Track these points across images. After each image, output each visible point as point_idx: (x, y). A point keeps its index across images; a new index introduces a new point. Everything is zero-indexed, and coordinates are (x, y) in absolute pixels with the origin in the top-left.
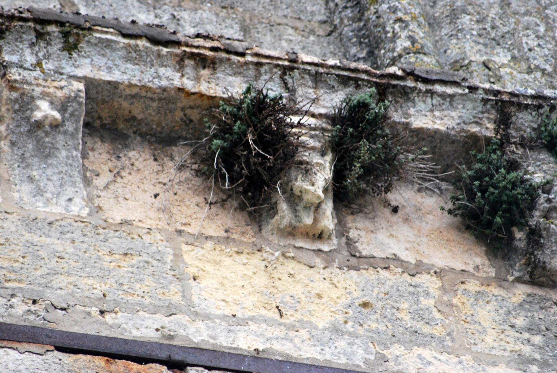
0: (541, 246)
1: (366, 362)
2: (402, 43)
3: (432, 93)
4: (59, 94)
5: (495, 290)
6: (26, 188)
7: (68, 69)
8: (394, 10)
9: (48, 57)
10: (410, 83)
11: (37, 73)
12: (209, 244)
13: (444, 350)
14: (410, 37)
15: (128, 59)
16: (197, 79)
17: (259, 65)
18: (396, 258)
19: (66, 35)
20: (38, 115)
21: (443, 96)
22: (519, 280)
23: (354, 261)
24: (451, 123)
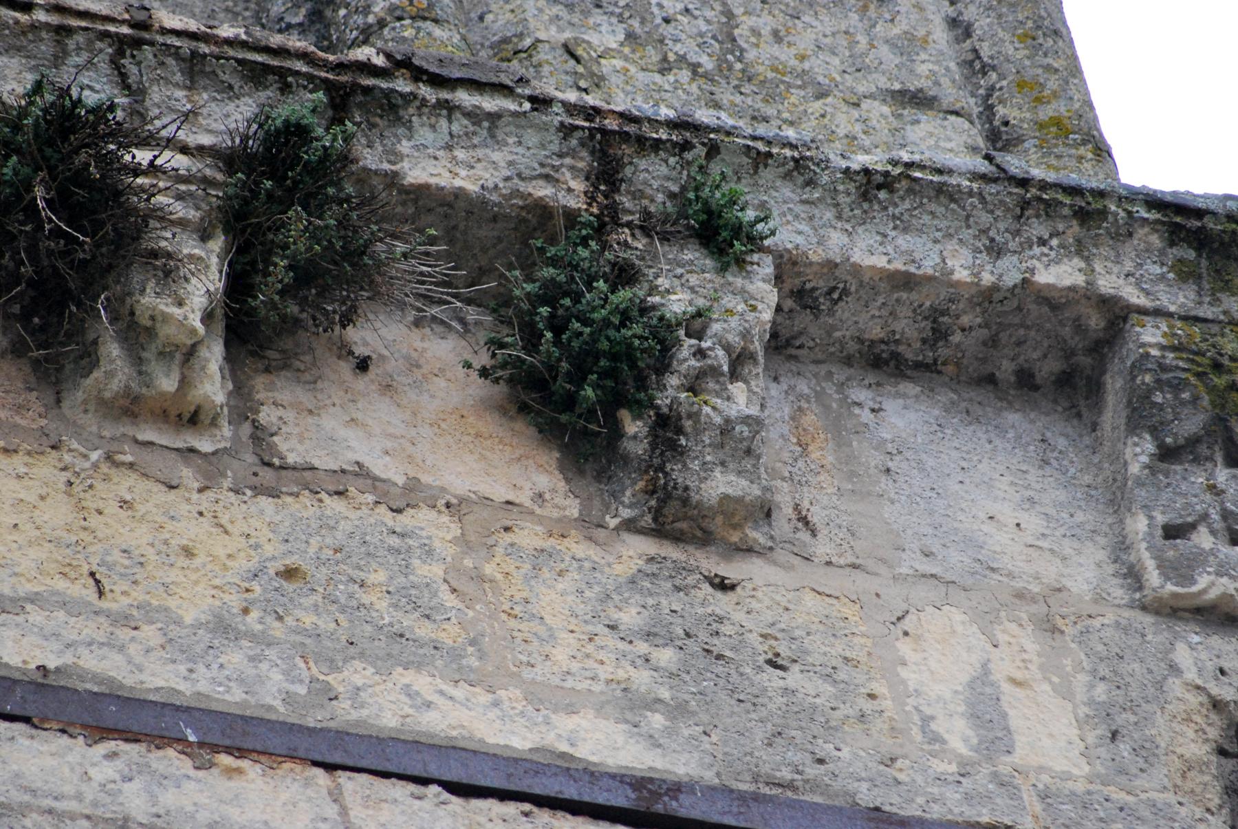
3: (449, 108)
5: (578, 547)
10: (403, 85)
17: (62, 31)
18: (361, 472)
21: (475, 116)
22: (630, 526)
23: (267, 475)
24: (491, 177)
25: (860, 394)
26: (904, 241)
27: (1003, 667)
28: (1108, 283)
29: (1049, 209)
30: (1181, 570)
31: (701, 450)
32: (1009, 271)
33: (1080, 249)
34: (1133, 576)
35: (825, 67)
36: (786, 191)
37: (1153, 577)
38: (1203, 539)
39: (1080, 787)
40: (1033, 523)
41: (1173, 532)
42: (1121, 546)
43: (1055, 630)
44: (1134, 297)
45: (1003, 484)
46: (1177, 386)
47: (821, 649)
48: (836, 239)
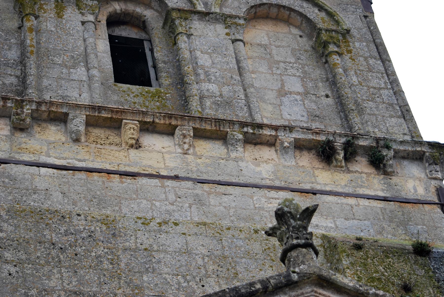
0: (386, 167)
1: (352, 192)
2: (357, 128)
3: (363, 138)
4: (289, 141)
5: (377, 176)
6: (283, 160)
7: (290, 136)
8: (355, 122)
9: (286, 134)
10: (359, 136)
11: (284, 137)
12: (320, 170)
13: (367, 188)
14: (358, 127)
15: (302, 133)
16: (316, 137)
17: (328, 133)
18: (357, 171)
19: (290, 129)
20: (285, 145)
21: (365, 138)
22: (382, 174)
23: (349, 172)
24: (367, 144)
25: (402, 161)
26: (405, 147)
27: (416, 185)
28: (423, 149)
29: (418, 143)
30: (431, 175)
31: (388, 167)
32: (414, 149)
33: (420, 147)
34: (427, 176)
35: (396, 132)
36: (394, 143)
37: (429, 176)
38: (433, 172)
39: (424, 195)
40: (418, 171)
41: (431, 171)
42: (426, 173)
43: (420, 181)
44: (426, 151)
45: (415, 168)
46: (430, 158)
47: (400, 184)
48: (399, 147)
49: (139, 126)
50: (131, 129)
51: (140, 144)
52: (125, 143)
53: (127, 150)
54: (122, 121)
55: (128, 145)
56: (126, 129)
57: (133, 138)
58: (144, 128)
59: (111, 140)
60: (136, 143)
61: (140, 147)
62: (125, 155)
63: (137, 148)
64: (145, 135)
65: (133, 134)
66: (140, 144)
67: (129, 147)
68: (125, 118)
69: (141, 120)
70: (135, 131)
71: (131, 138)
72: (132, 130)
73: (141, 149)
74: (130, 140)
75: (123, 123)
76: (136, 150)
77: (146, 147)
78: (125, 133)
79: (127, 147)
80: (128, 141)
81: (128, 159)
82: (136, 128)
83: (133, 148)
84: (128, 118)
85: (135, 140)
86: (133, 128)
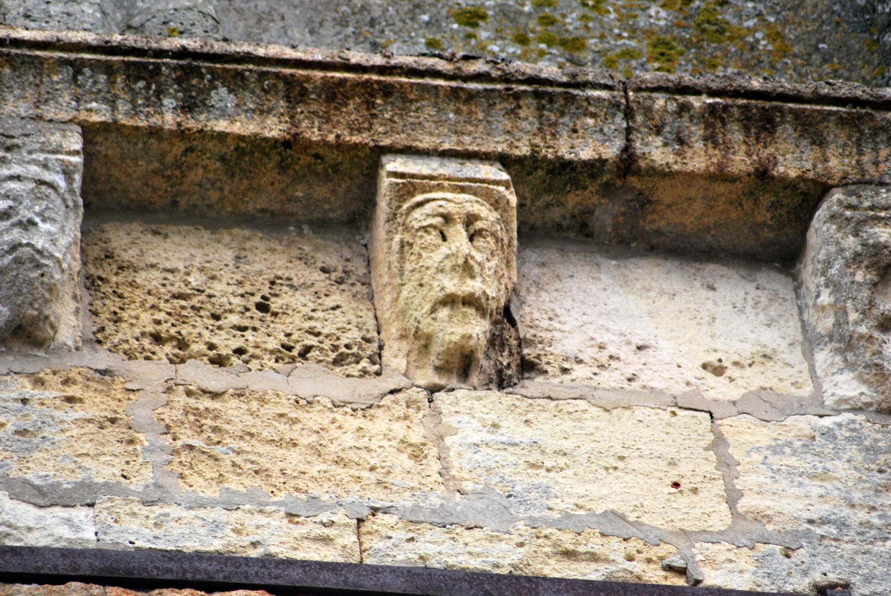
49: (513, 200)
50: (450, 232)
51: (530, 343)
52: (405, 346)
53: (423, 395)
54: (375, 167)
55: (433, 359)
56: (407, 229)
57: (470, 301)
58: (556, 214)
59: (294, 323)
60: (496, 342)
61: (528, 367)
62: (415, 438)
63: (502, 382)
64: (562, 270)
65: (467, 269)
66: (530, 343)
67: (438, 369)
68: (401, 139)
69: (524, 150)
70: (480, 242)
71: (450, 301)
72: (458, 236)
73: (535, 385)
74: (444, 313)
75: (385, 183)
76: (495, 394)
77: (579, 372)
78: (402, 259)
79: (427, 376)
80: (427, 325)
81: (436, 466)
82: (488, 215)
83: (475, 379)
84: (426, 142)
85: (482, 311)
86: (470, 220)
